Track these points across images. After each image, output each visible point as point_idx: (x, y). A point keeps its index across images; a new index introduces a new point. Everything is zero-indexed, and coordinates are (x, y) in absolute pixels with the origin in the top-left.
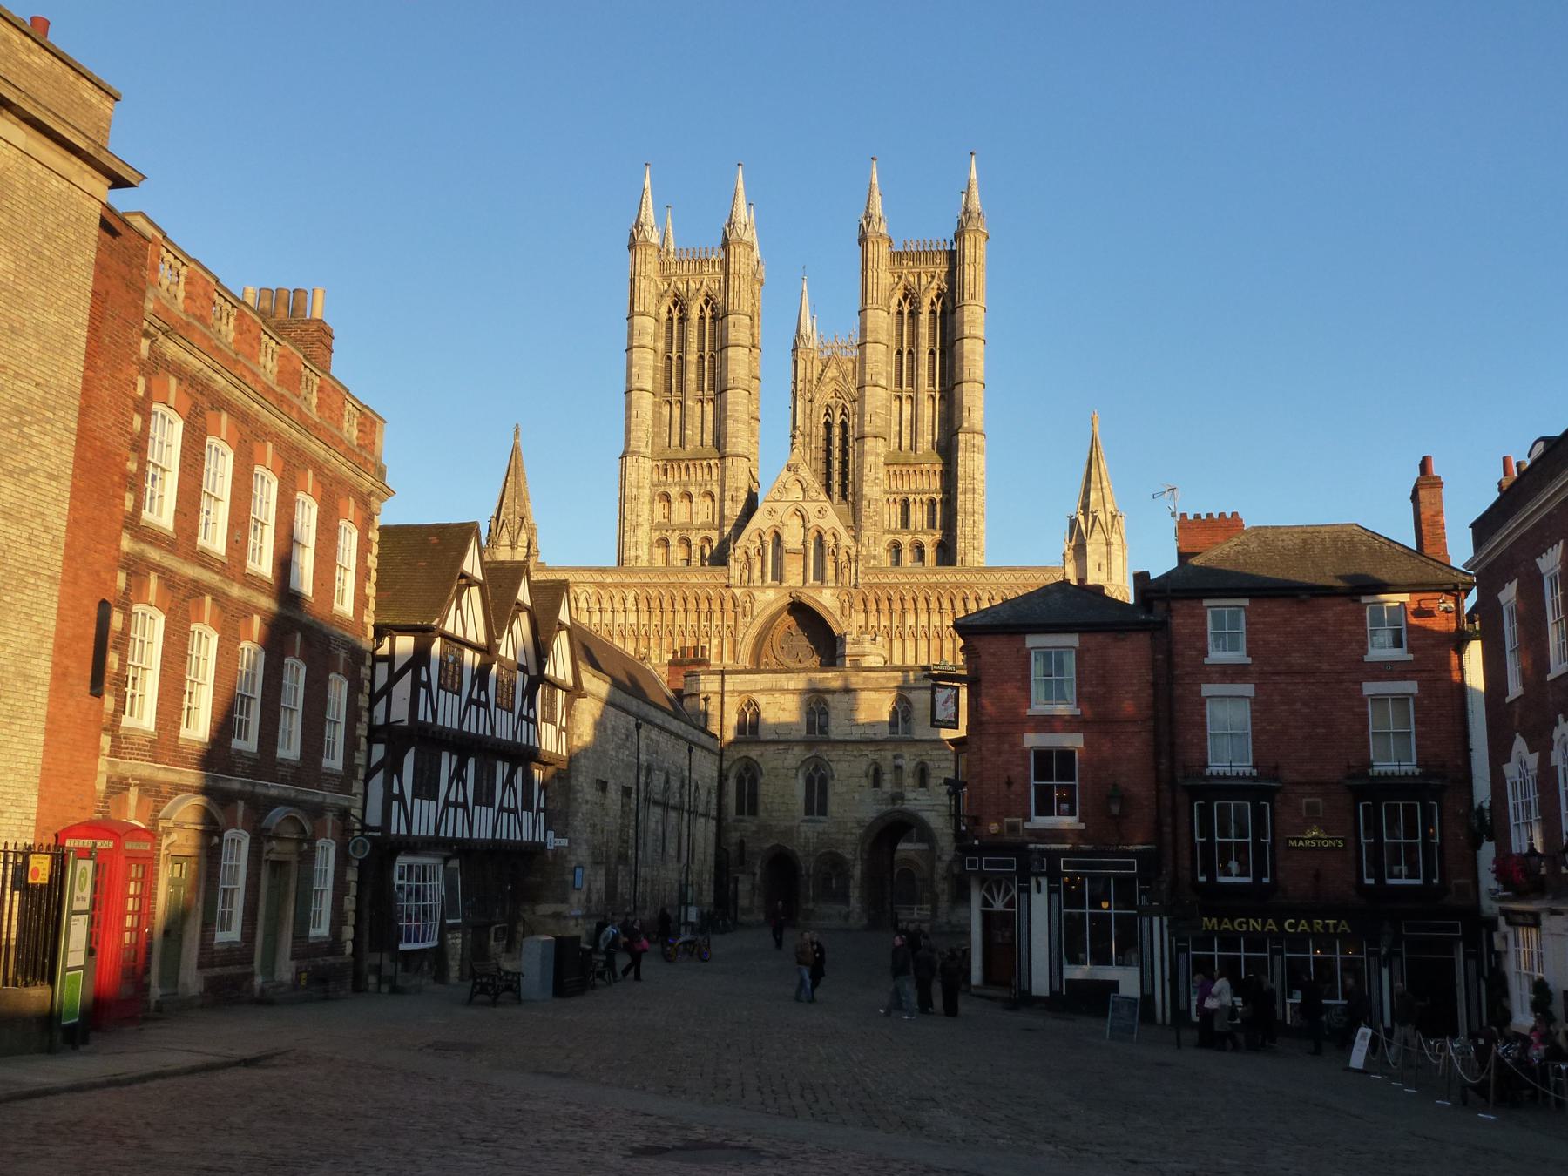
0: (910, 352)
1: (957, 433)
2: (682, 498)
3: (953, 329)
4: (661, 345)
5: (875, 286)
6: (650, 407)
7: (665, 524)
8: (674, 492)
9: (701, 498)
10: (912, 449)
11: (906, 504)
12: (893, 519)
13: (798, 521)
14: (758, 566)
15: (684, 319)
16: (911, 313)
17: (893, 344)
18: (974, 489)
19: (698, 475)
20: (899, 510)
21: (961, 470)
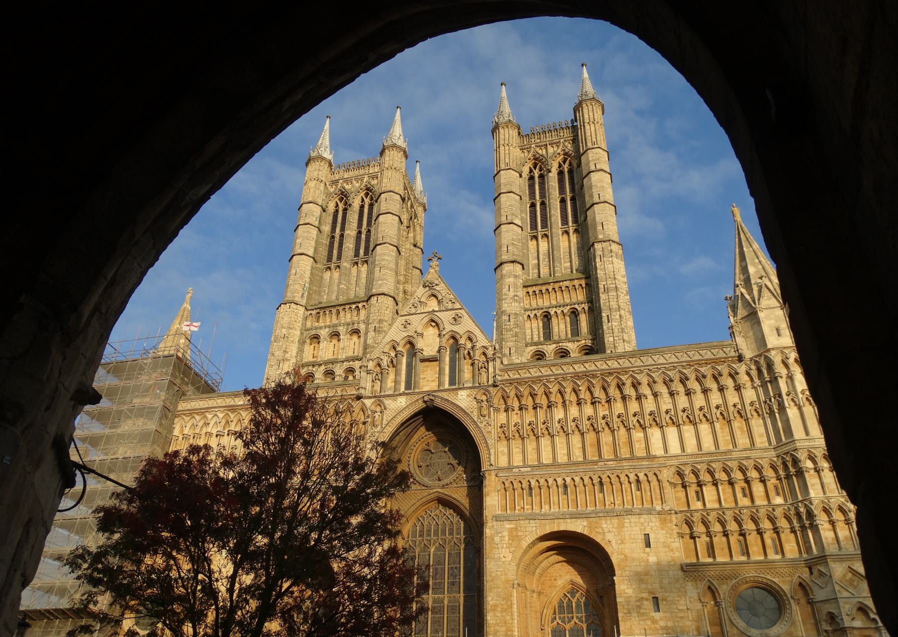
0: (543, 204)
1: (593, 244)
2: (331, 338)
3: (583, 197)
4: (327, 228)
5: (507, 156)
6: (309, 268)
7: (313, 362)
8: (324, 333)
9: (348, 336)
10: (551, 276)
11: (547, 317)
12: (536, 333)
13: (432, 332)
14: (392, 376)
15: (347, 206)
16: (541, 177)
17: (526, 198)
18: (616, 287)
19: (347, 317)
20: (541, 325)
21: (600, 273)
